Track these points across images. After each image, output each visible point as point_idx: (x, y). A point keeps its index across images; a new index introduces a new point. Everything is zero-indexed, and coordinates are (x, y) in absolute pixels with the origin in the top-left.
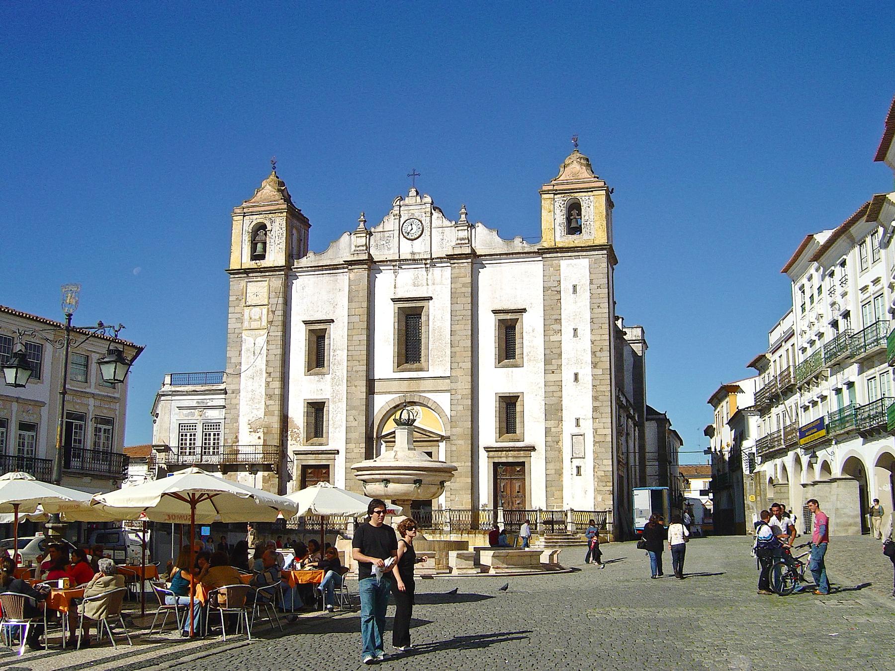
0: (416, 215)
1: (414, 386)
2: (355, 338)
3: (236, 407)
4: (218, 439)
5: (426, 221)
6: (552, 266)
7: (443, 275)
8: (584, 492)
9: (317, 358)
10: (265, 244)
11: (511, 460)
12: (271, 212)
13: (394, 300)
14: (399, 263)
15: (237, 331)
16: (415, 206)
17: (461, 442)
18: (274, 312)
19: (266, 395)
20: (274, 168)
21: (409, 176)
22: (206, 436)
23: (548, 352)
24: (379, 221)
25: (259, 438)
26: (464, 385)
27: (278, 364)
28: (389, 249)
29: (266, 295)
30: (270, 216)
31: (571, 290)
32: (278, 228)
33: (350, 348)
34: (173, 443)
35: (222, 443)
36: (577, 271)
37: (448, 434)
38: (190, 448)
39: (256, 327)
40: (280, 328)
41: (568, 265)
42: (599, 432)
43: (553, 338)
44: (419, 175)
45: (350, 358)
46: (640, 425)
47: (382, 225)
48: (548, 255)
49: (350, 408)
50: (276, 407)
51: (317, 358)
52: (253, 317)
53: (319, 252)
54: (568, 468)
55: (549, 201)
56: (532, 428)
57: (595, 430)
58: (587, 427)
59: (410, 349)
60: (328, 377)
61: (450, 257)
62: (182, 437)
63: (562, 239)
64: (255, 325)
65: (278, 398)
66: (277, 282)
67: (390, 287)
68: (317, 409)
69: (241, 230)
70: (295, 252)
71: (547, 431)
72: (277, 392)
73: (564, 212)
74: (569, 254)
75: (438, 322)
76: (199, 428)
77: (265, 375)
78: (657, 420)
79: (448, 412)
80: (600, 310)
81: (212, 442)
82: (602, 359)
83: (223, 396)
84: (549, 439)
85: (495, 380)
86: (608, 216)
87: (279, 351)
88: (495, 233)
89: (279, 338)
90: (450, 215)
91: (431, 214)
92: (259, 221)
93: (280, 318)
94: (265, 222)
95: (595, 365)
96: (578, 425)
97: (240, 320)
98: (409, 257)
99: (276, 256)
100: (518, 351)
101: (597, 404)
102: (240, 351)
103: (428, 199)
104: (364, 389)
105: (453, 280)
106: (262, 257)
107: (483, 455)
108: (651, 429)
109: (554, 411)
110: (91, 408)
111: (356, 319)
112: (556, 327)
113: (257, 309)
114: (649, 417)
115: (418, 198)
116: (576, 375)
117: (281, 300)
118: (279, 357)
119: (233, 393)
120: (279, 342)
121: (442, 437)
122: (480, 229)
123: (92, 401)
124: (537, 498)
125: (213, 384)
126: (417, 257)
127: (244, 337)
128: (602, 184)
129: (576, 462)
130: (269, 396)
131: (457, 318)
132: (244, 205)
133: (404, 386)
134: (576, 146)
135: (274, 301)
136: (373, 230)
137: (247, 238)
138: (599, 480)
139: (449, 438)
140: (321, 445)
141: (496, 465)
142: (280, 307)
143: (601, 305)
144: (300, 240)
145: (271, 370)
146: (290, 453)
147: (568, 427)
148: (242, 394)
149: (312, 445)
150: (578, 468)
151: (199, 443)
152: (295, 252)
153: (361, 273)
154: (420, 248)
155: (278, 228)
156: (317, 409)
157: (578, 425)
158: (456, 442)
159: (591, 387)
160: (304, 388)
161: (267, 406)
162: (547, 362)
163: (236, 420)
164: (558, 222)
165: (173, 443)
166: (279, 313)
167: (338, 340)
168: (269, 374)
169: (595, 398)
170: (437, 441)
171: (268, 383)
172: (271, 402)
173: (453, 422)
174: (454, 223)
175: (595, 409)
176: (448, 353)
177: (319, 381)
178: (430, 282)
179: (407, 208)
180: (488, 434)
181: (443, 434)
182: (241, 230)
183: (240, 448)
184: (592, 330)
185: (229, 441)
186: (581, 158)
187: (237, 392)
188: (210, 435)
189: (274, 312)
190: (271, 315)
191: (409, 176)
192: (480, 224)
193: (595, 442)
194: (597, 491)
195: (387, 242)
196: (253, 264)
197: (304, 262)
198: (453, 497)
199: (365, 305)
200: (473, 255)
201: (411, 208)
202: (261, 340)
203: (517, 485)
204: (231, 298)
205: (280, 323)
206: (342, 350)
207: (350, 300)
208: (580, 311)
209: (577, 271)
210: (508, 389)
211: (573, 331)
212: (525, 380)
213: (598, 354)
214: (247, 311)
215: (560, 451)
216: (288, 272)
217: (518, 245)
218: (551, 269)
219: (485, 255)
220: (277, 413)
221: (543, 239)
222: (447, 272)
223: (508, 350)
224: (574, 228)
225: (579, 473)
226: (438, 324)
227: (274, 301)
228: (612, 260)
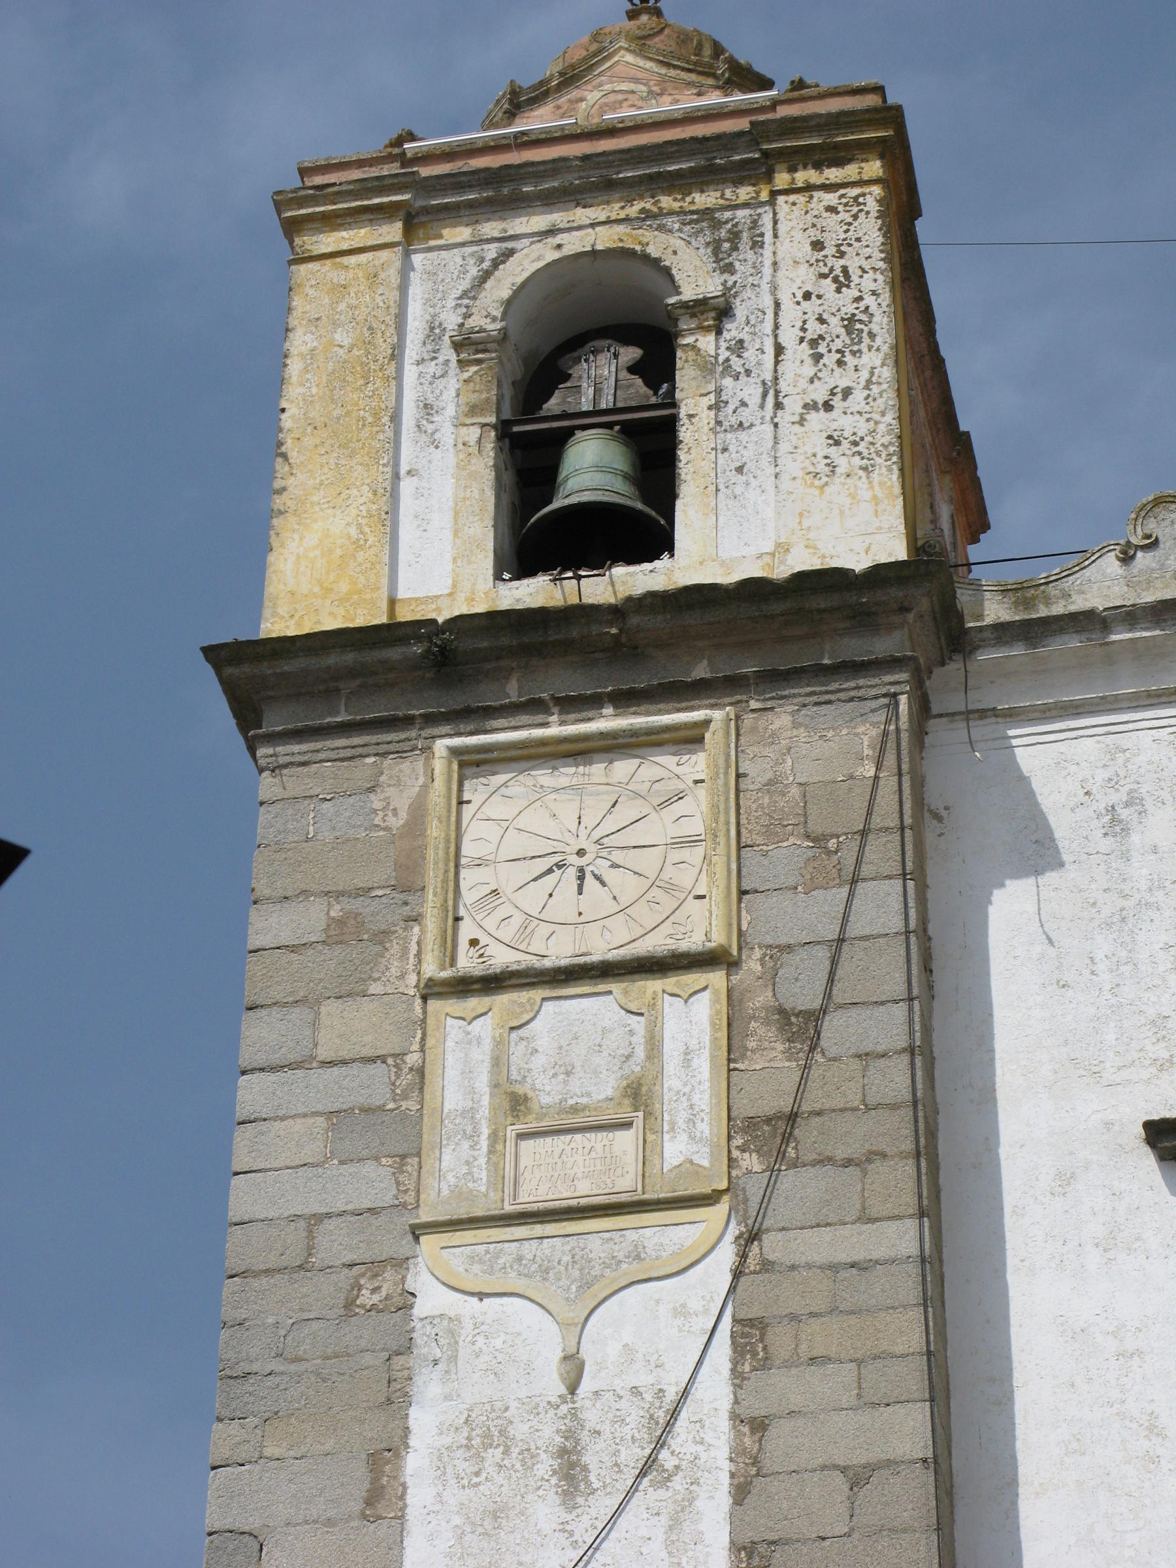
15: (336, 1244)
18: (803, 1028)
39: (586, 1190)
40: (897, 1180)
52: (547, 1092)
92: (574, 243)
94: (656, 244)
102: (385, 1457)
113: (597, 1010)
117: (881, 907)
127: (432, 1301)
204: (268, 927)
214: (465, 1042)
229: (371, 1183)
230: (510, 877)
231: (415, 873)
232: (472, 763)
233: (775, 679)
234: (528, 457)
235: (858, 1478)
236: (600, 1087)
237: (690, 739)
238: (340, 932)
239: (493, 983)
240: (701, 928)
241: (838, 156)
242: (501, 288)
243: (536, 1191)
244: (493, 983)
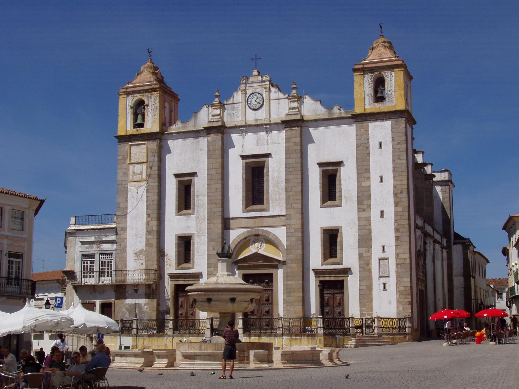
0: (258, 90)
1: (258, 222)
2: (213, 186)
3: (124, 240)
4: (111, 265)
5: (265, 94)
6: (362, 127)
7: (280, 137)
8: (388, 303)
9: (185, 202)
10: (143, 115)
11: (332, 279)
12: (147, 91)
13: (243, 157)
14: (245, 129)
15: (124, 183)
16: (256, 84)
17: (294, 265)
18: (151, 168)
19: (147, 231)
20: (150, 56)
21: (252, 59)
22: (102, 263)
23: (360, 194)
24: (230, 95)
25: (142, 264)
26: (296, 222)
27: (155, 207)
28: (238, 117)
29: (145, 155)
30: (147, 94)
31: (378, 146)
32: (153, 103)
33: (209, 194)
34: (77, 269)
35: (114, 268)
36: (381, 132)
37: (285, 260)
38: (90, 273)
39: (138, 179)
41: (375, 126)
42: (401, 256)
43: (364, 184)
44: (260, 59)
45: (210, 202)
46: (449, 248)
47: (232, 99)
49: (210, 240)
50: (154, 240)
51: (185, 202)
52: (136, 172)
53: (185, 121)
54: (377, 284)
55: (359, 77)
56: (349, 255)
57: (397, 255)
58: (391, 253)
60: (193, 217)
64: (137, 178)
65: (155, 233)
68: (185, 243)
69: (126, 105)
70: (167, 121)
71: (361, 256)
72: (155, 229)
73: (372, 85)
75: (276, 172)
76: (97, 257)
77: (145, 216)
78: (463, 244)
79: (284, 242)
80: (399, 161)
81: (106, 267)
82: (402, 199)
84: (362, 262)
85: (320, 218)
86: (406, 87)
87: (156, 198)
88: (319, 103)
89: (156, 188)
91: (270, 89)
92: (139, 98)
93: (156, 172)
95: (396, 204)
96: (384, 251)
97: (126, 174)
98: (253, 123)
99: (151, 124)
100: (337, 194)
101: (399, 234)
102: (127, 198)
103: (267, 78)
104: (220, 226)
105: (287, 140)
106: (142, 125)
107: (312, 275)
108: (457, 250)
109: (365, 240)
110: (5, 246)
111: (213, 172)
112: (366, 175)
113: (139, 165)
114: (457, 241)
115: (260, 77)
116: (382, 212)
117: (156, 159)
118: (156, 202)
119: (122, 230)
120: (156, 191)
121: (279, 261)
122: (308, 101)
123: (5, 241)
124: (353, 309)
125: (106, 223)
126: (259, 122)
128: (400, 62)
129: (383, 280)
130: (149, 232)
131: (290, 170)
132: (128, 86)
133: (251, 222)
134: (382, 32)
135: (151, 159)
136: (225, 102)
137: (130, 112)
138: (400, 293)
139: (284, 262)
140: (189, 268)
141: (321, 282)
142: (156, 164)
143: (401, 157)
144: (171, 111)
145: (150, 212)
147: (376, 253)
148: (129, 231)
149: (182, 268)
150: (384, 284)
151: (97, 268)
152: (167, 121)
153: (217, 137)
154: (261, 116)
155: (153, 102)
156: (185, 243)
157: (384, 251)
158: (289, 265)
159: (393, 221)
160: (176, 225)
161: (147, 240)
162: (360, 202)
163: (124, 250)
164: (367, 93)
165: (77, 269)
166: (155, 168)
167: (200, 187)
168: (148, 215)
169: (397, 230)
170: (277, 264)
171: (148, 223)
172: (151, 237)
173: (288, 250)
174: (287, 96)
175: (397, 238)
176: (284, 196)
177: (186, 220)
178: (269, 142)
179: (251, 85)
180: (316, 259)
181: (281, 259)
182: (126, 105)
183: (128, 272)
184: (394, 177)
185: (120, 267)
186: (384, 42)
187: (125, 229)
188: (105, 262)
189: (151, 168)
190: (149, 170)
191: (252, 59)
192: (307, 96)
193: (397, 265)
194: (399, 302)
195: (236, 113)
196: (134, 131)
197: (174, 129)
198: (288, 308)
199: (220, 160)
200: (302, 120)
201: (254, 85)
202: (143, 189)
203: (338, 297)
205: (156, 176)
206: (204, 196)
207: (209, 157)
208: (384, 163)
209: (381, 132)
211: (379, 178)
212: (343, 216)
213: (399, 195)
214: (131, 167)
215: (370, 271)
218: (362, 130)
219: (312, 121)
220: (155, 245)
221: (356, 107)
222: (282, 134)
223: (330, 192)
224: (379, 96)
225: (384, 288)
226: (276, 174)
227: (151, 159)
228: (411, 121)
229: (125, 178)
230: (134, 155)
231: (128, 154)
232: (131, 145)
233: (150, 140)
234: (135, 115)
235: (153, 201)
236: (139, 172)
237: (145, 144)
238: (123, 158)
239: (132, 164)
240: (145, 160)
241: (156, 91)
242: (133, 102)
243: (135, 180)
244: (132, 164)
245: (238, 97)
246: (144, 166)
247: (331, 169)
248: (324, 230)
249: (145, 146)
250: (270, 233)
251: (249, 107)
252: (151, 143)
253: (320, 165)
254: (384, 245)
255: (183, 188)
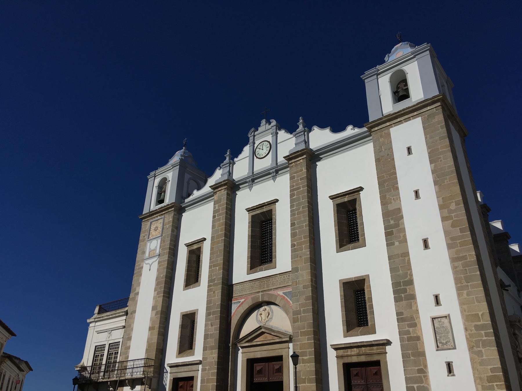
4: (117, 357)
22: (109, 354)
24: (240, 151)
48: (376, 129)
58: (451, 306)
59: (262, 252)
61: (289, 158)
62: (95, 356)
63: (388, 106)
66: (169, 218)
67: (246, 200)
74: (399, 120)
83: (124, 318)
85: (339, 266)
90: (291, 129)
97: (144, 253)
99: (169, 198)
107: (332, 355)
109: (403, 288)
146: (166, 366)
147: (426, 310)
150: (449, 366)
210: (352, 274)
216: (179, 209)
217: (350, 131)
245: (247, 150)
246: (159, 241)
247: (348, 201)
248: (343, 283)
249: (161, 221)
250: (276, 296)
251: (257, 158)
252: (166, 215)
253: (332, 198)
254: (436, 293)
255: (194, 258)
